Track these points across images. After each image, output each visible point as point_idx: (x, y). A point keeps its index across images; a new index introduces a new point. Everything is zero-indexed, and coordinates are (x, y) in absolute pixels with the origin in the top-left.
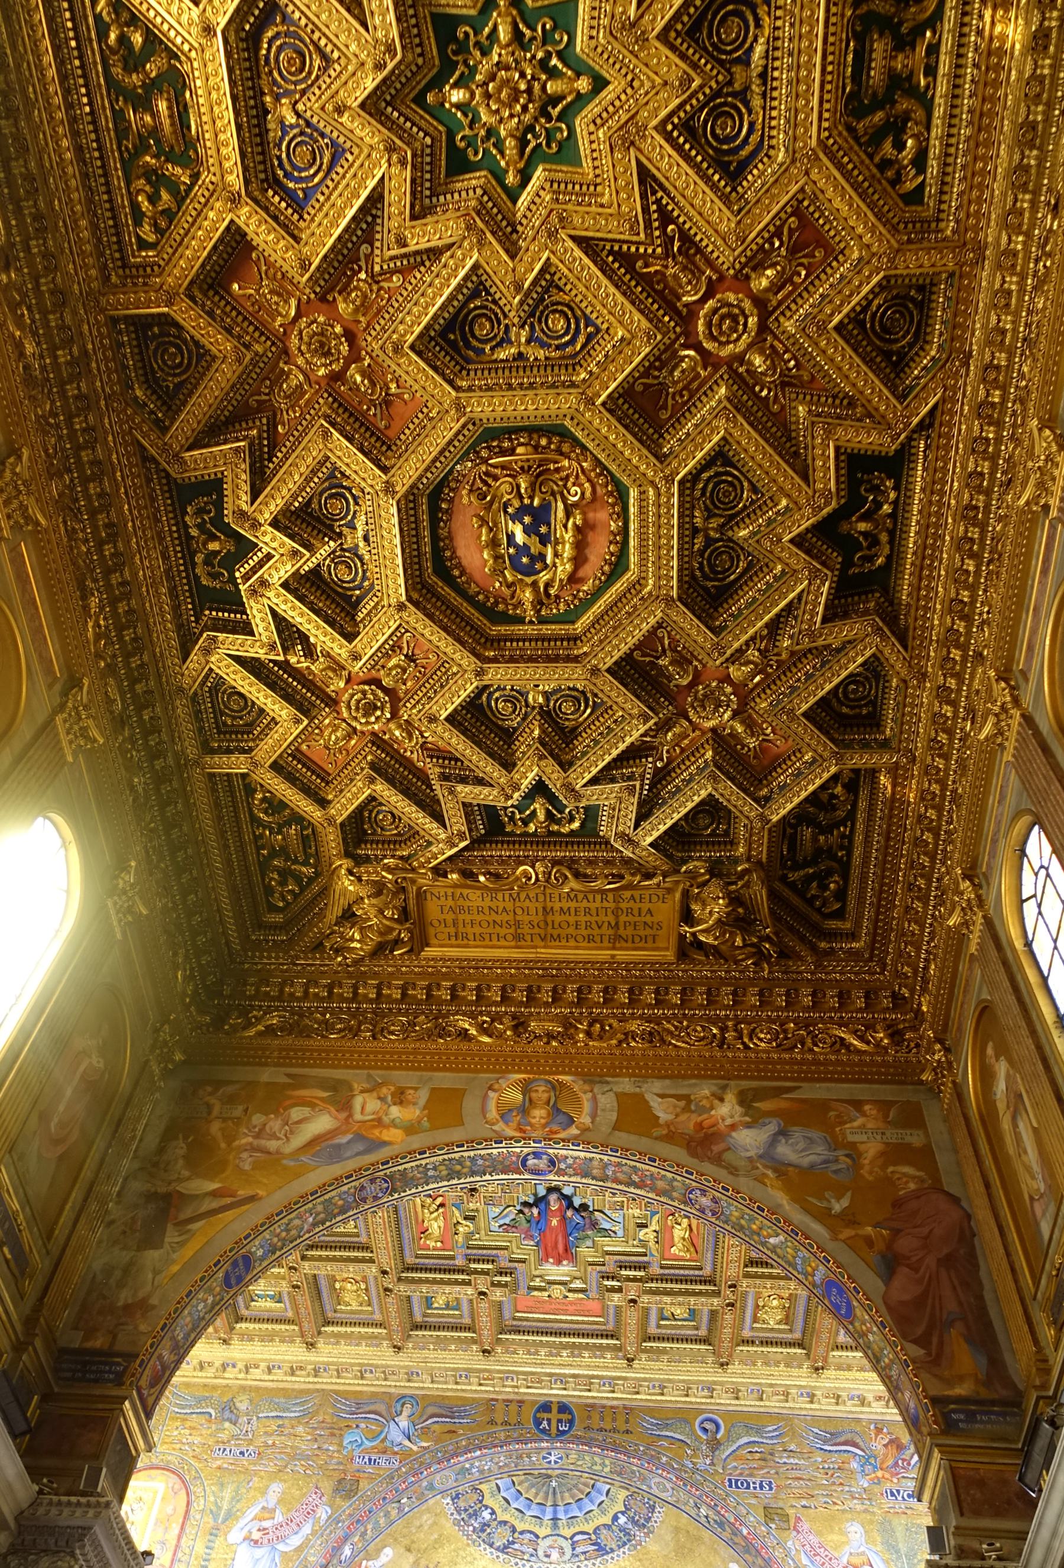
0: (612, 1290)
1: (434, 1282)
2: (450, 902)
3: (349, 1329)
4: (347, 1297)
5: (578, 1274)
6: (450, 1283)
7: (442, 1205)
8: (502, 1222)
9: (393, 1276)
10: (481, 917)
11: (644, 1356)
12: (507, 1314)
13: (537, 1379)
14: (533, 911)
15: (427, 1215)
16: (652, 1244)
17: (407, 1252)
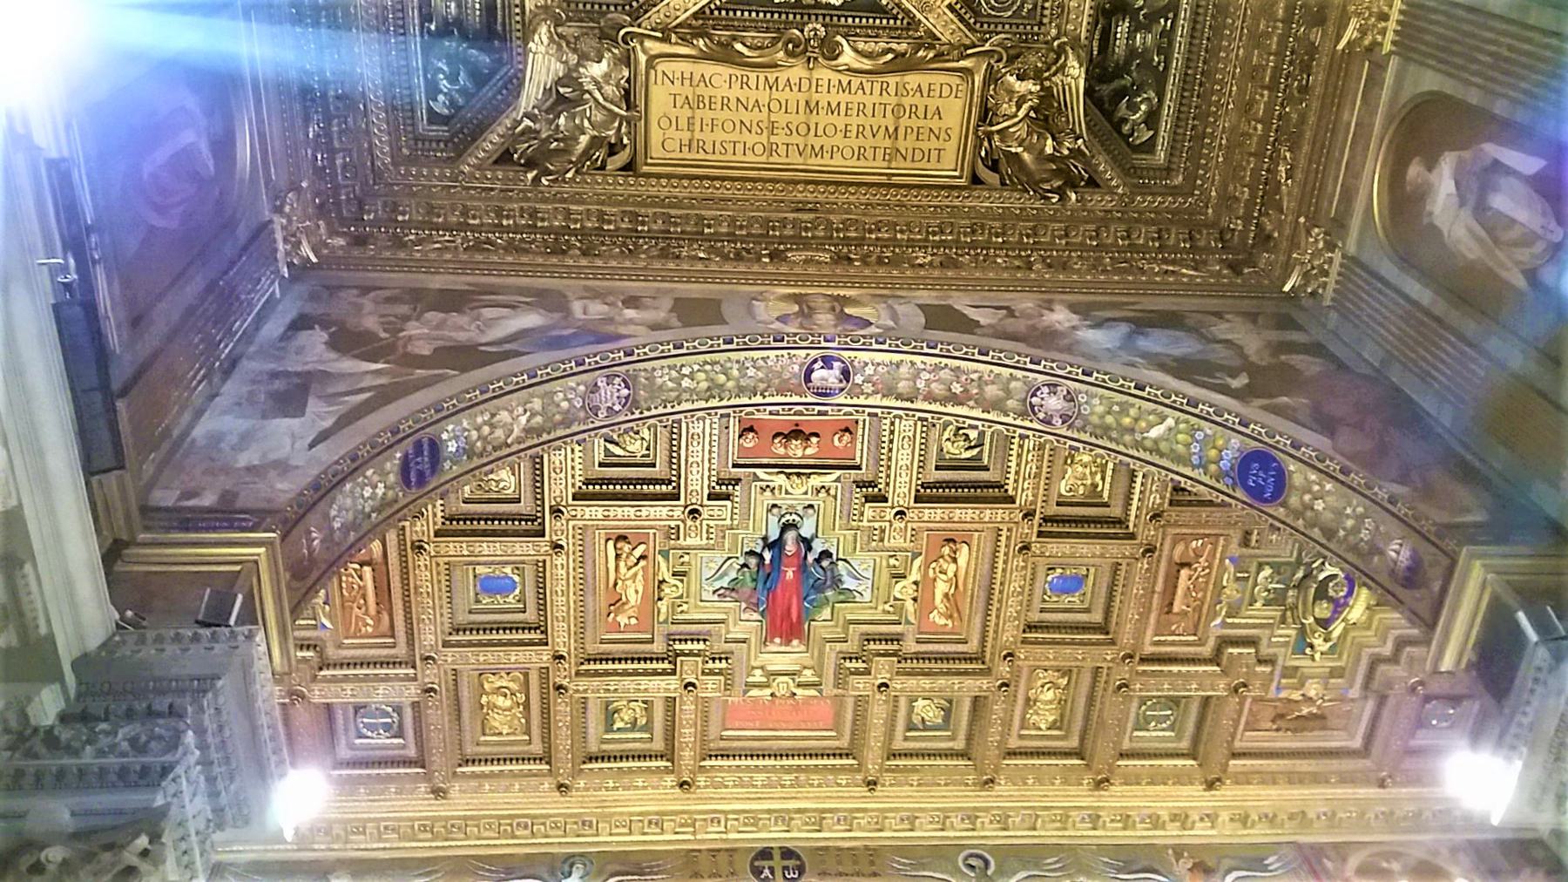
0: (857, 672)
1: (625, 673)
2: (687, 90)
3: (496, 768)
4: (497, 721)
5: (809, 662)
6: (646, 673)
7: (643, 557)
8: (717, 585)
9: (569, 666)
10: (726, 114)
11: (888, 778)
12: (713, 731)
13: (753, 819)
14: (792, 108)
15: (623, 569)
16: (909, 605)
17: (589, 634)
